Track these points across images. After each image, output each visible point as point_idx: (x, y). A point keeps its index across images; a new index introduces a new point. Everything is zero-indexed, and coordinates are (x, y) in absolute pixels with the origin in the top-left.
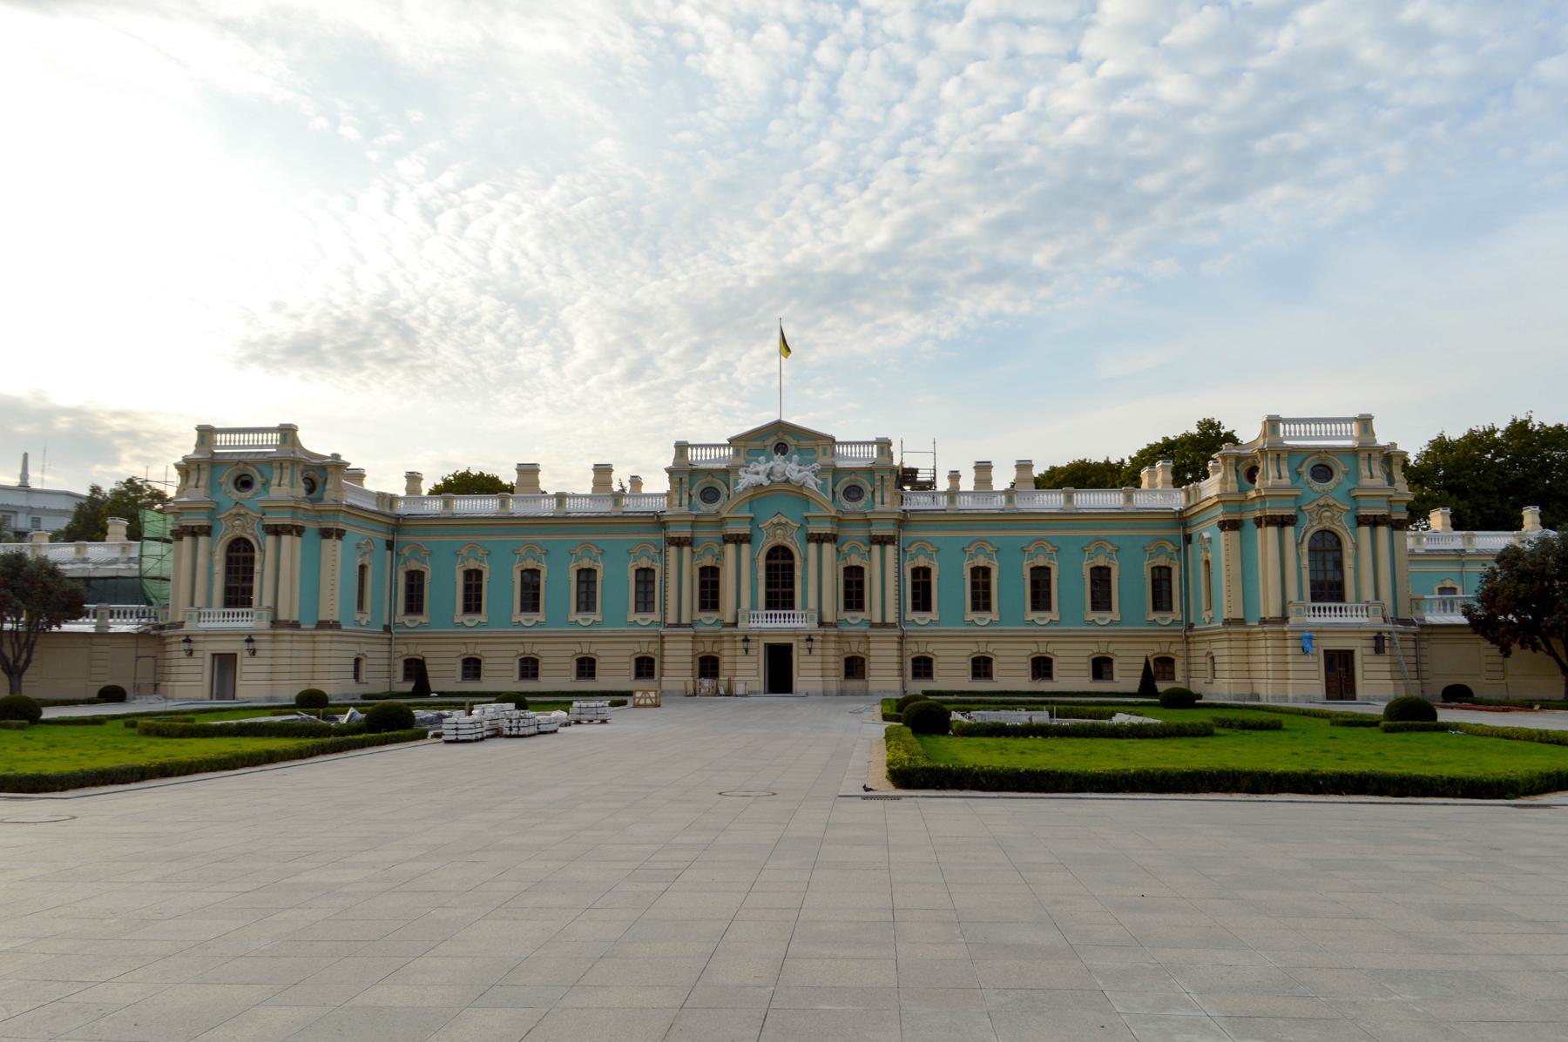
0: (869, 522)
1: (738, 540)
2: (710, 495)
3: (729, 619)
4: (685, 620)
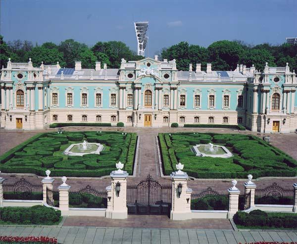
0: (170, 84)
1: (139, 89)
2: (130, 76)
3: (136, 108)
4: (124, 108)
